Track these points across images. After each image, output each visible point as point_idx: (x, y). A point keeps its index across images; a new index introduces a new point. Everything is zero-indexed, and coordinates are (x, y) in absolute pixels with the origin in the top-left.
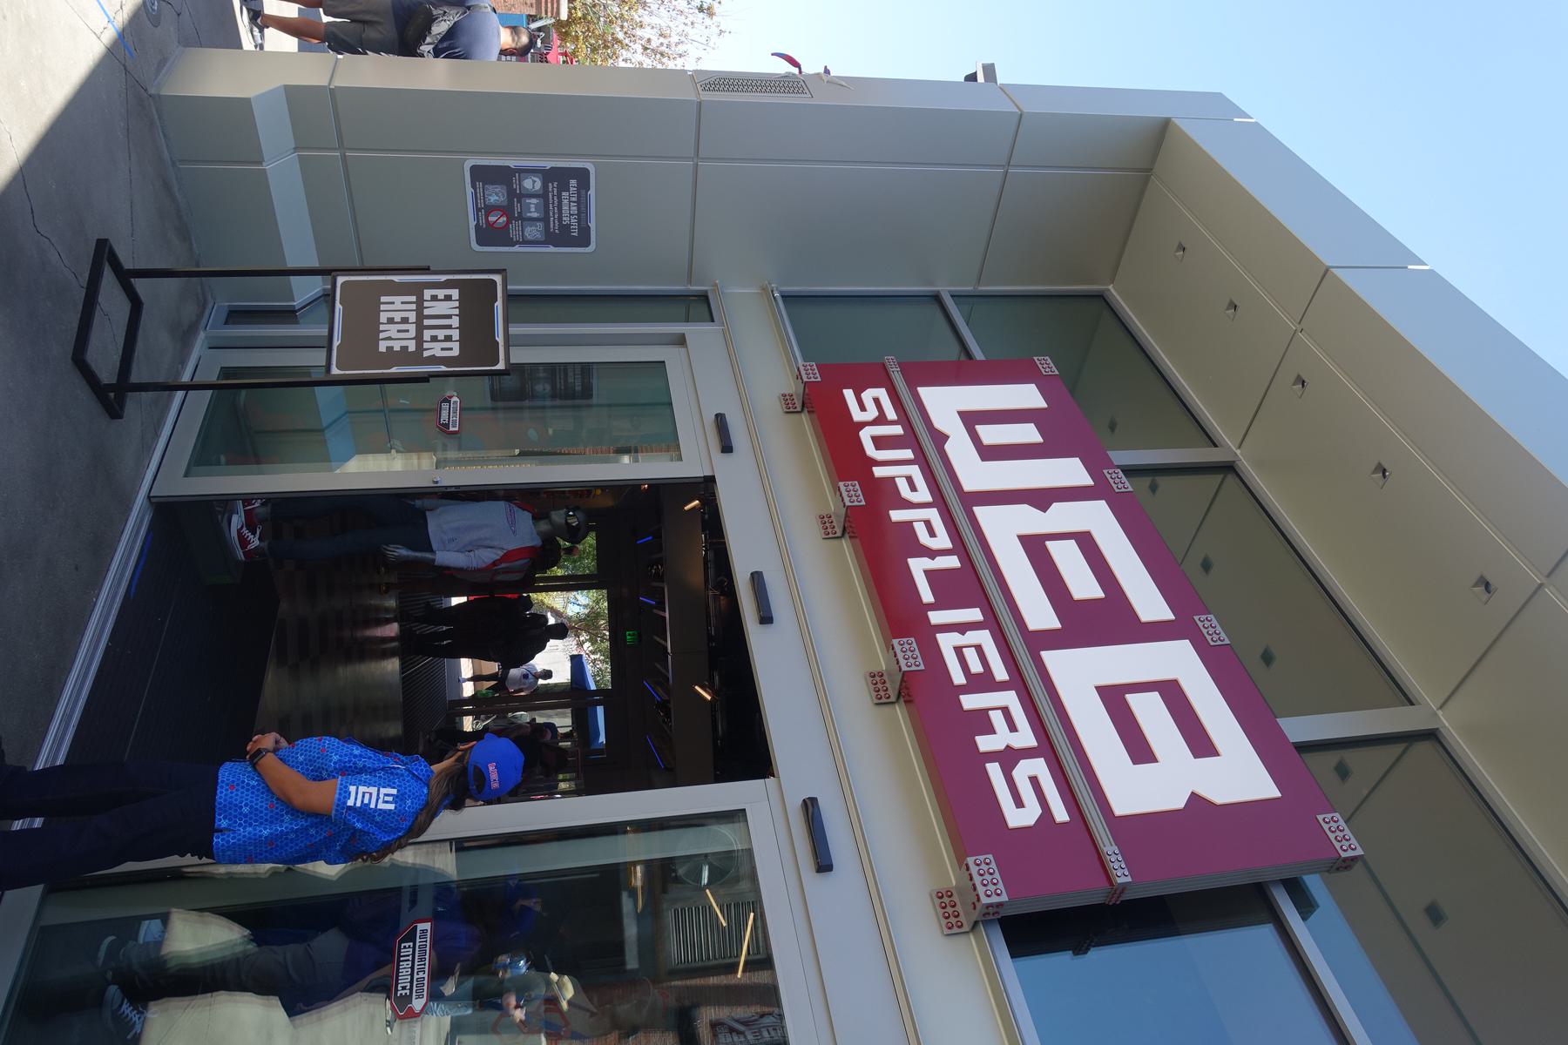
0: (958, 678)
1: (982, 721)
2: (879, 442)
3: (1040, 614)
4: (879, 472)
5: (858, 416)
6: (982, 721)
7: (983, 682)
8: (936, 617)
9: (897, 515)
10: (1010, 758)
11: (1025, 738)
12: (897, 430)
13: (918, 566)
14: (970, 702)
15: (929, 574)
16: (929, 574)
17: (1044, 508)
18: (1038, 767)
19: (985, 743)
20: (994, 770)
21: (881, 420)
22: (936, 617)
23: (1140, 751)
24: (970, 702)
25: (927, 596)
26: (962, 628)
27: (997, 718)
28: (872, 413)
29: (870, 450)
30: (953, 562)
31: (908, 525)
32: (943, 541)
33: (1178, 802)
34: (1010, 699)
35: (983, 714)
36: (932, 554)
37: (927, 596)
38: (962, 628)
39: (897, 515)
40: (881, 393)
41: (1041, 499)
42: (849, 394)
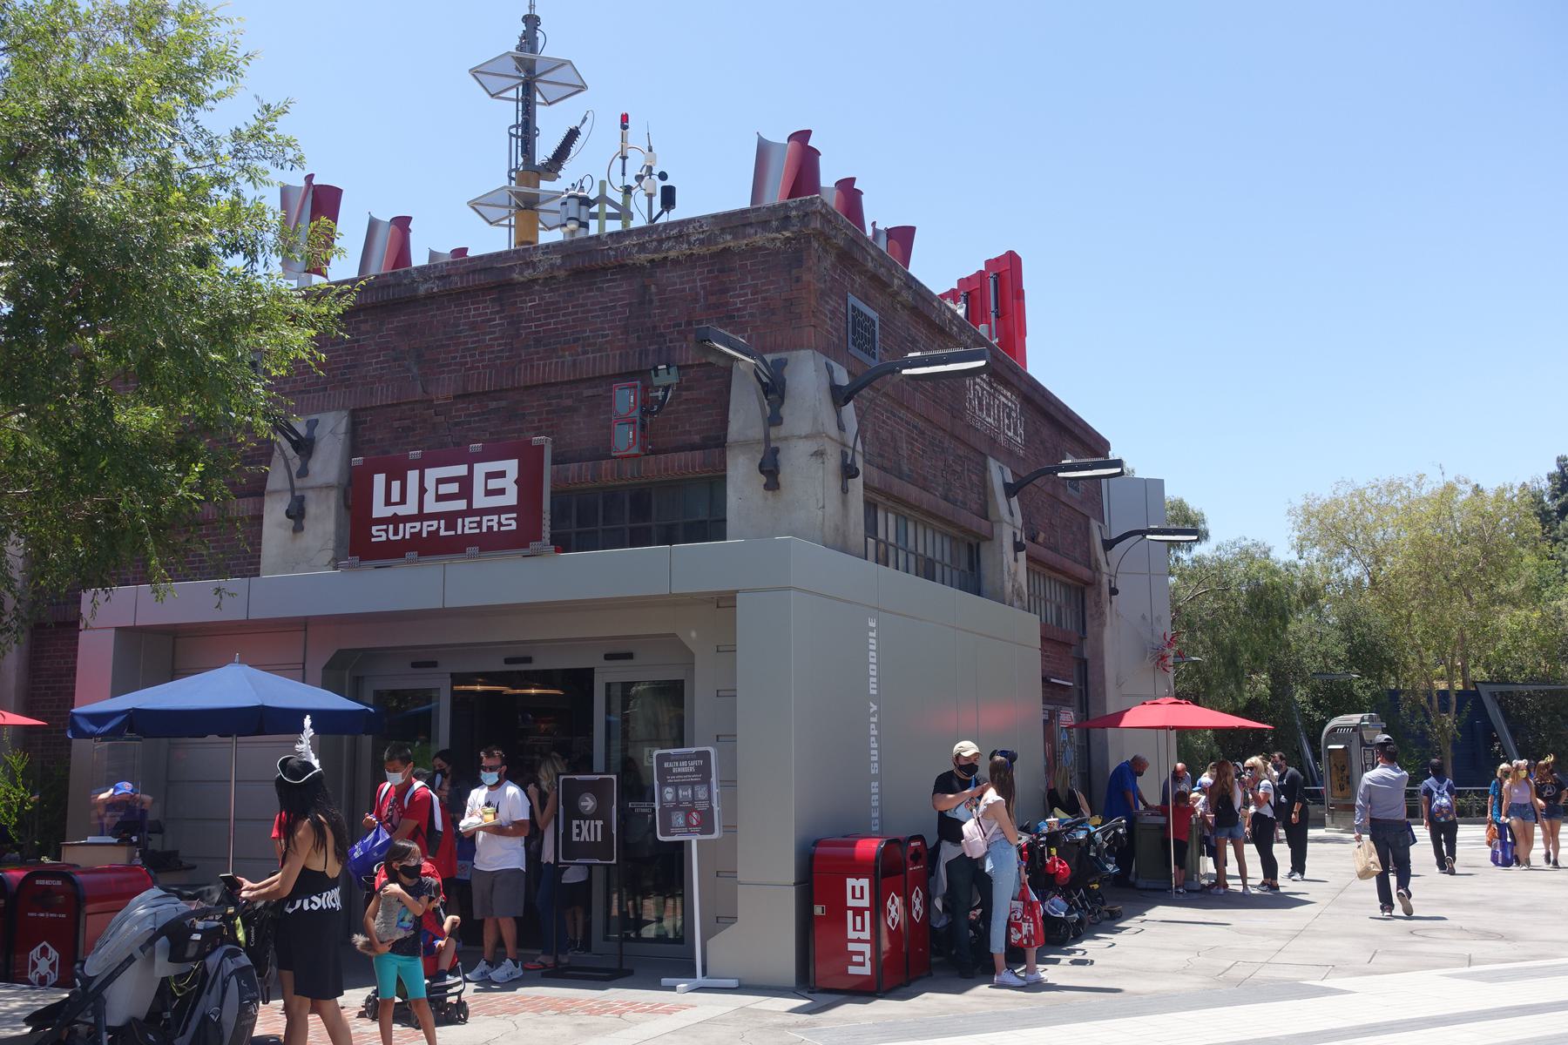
0: (478, 531)
1: (490, 528)
2: (396, 533)
3: (461, 505)
4: (407, 536)
5: (384, 538)
6: (490, 528)
7: (480, 524)
8: (459, 532)
9: (424, 535)
10: (500, 524)
11: (495, 518)
12: (391, 527)
13: (442, 533)
14: (484, 530)
15: (446, 530)
16: (446, 530)
17: (426, 491)
18: (503, 517)
19: (495, 529)
20: (502, 529)
21: (386, 531)
22: (459, 532)
23: (501, 492)
24: (484, 530)
25: (453, 533)
26: (463, 526)
27: (490, 524)
28: (383, 533)
29: (399, 537)
30: (442, 522)
31: (428, 532)
32: (435, 523)
33: (516, 487)
34: (485, 518)
35: (488, 527)
36: (439, 528)
37: (453, 533)
38: (463, 526)
39: (424, 535)
40: (374, 529)
41: (422, 491)
42: (373, 540)
